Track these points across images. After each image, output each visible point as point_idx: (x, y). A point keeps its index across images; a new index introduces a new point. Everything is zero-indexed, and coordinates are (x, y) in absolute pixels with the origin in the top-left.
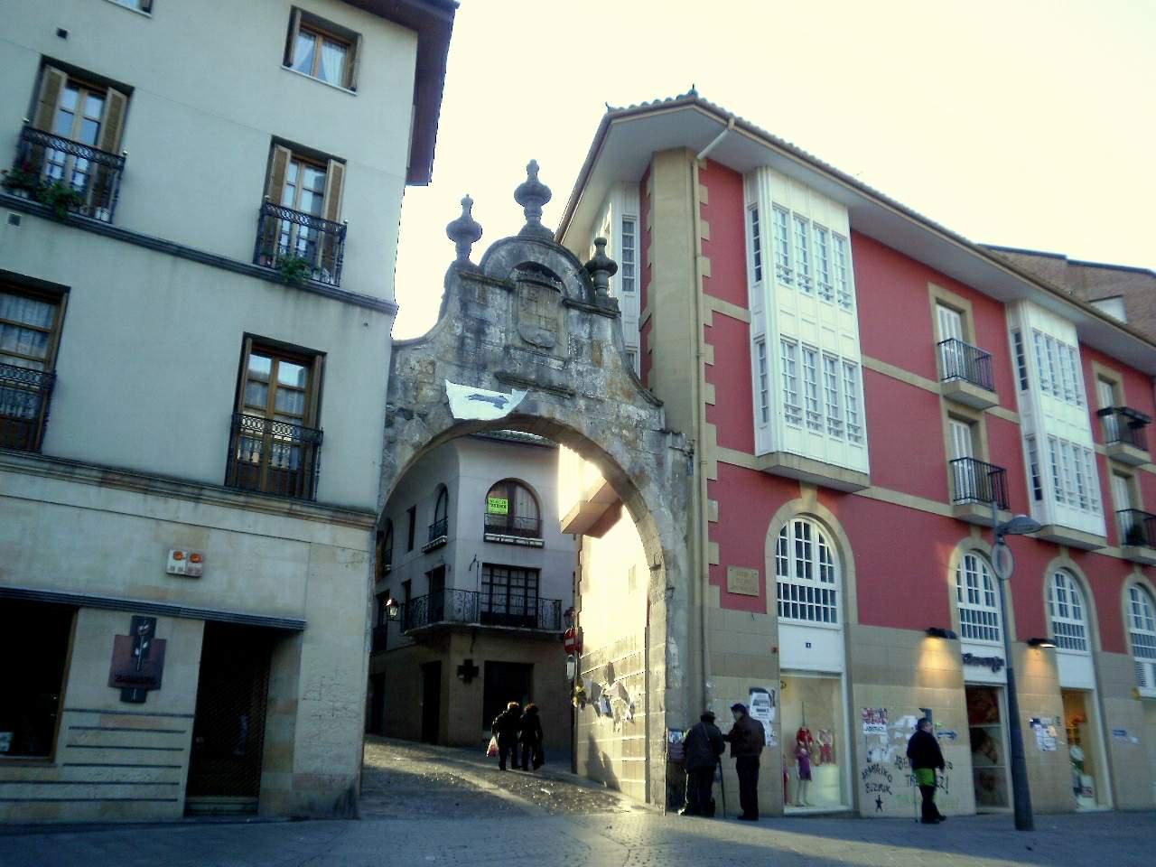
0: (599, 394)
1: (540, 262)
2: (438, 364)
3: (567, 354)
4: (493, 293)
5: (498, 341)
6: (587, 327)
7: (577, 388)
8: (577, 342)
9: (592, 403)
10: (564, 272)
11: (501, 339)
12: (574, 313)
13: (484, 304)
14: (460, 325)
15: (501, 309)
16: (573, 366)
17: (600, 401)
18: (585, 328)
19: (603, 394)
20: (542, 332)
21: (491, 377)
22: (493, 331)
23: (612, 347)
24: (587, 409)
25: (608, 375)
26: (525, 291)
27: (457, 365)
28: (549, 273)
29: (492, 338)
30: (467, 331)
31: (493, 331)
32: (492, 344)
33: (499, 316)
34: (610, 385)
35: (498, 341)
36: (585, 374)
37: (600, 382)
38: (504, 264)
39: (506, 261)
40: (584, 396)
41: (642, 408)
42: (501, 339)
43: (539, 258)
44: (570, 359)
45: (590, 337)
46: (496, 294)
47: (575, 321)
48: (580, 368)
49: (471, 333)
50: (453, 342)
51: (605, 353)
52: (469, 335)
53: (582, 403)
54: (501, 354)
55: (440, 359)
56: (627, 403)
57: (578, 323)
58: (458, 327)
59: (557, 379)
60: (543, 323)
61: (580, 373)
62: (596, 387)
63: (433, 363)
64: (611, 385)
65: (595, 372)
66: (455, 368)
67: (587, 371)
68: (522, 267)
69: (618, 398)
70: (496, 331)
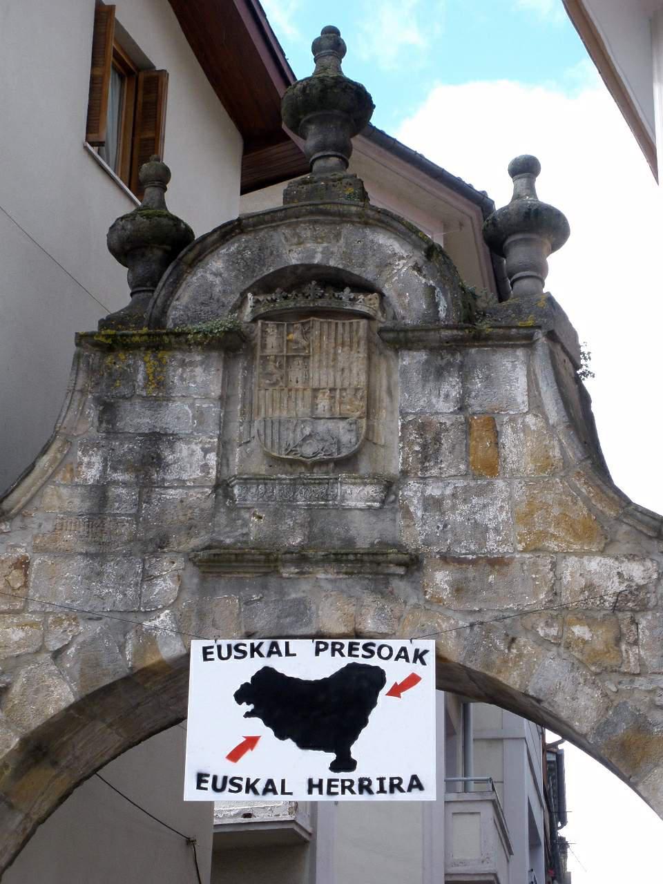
0: (493, 545)
1: (317, 260)
2: (36, 562)
3: (395, 466)
4: (183, 364)
5: (198, 474)
6: (452, 386)
7: (427, 543)
8: (422, 428)
9: (471, 572)
10: (386, 264)
11: (205, 468)
12: (412, 360)
13: (160, 392)
14: (97, 460)
15: (206, 397)
16: (411, 491)
17: (497, 563)
18: (445, 388)
19: (504, 542)
20: (322, 427)
21: (180, 563)
22: (185, 453)
23: (530, 420)
24: (459, 590)
25: (519, 491)
26: (272, 339)
27: (86, 554)
28: (334, 280)
29: (182, 469)
30: (115, 469)
31: (185, 453)
32: (182, 484)
33: (200, 416)
34: (524, 518)
35: (198, 474)
36: (448, 503)
37: (495, 513)
39: (224, 282)
40: (447, 559)
41: (632, 557)
42: (205, 468)
44: (405, 473)
45: (462, 408)
46: (191, 363)
47: (415, 377)
48: (434, 490)
49: (126, 470)
50: (77, 501)
51: (508, 438)
52: (118, 476)
53: (441, 578)
54: (209, 504)
55: (38, 549)
56: (580, 554)
57: (425, 380)
58: (90, 465)
59: (365, 532)
60: (323, 404)
61: (433, 504)
62: (487, 529)
63: (23, 565)
64: (530, 514)
65: (481, 492)
66: (80, 563)
67: (454, 495)
68: (265, 286)
69: (552, 545)
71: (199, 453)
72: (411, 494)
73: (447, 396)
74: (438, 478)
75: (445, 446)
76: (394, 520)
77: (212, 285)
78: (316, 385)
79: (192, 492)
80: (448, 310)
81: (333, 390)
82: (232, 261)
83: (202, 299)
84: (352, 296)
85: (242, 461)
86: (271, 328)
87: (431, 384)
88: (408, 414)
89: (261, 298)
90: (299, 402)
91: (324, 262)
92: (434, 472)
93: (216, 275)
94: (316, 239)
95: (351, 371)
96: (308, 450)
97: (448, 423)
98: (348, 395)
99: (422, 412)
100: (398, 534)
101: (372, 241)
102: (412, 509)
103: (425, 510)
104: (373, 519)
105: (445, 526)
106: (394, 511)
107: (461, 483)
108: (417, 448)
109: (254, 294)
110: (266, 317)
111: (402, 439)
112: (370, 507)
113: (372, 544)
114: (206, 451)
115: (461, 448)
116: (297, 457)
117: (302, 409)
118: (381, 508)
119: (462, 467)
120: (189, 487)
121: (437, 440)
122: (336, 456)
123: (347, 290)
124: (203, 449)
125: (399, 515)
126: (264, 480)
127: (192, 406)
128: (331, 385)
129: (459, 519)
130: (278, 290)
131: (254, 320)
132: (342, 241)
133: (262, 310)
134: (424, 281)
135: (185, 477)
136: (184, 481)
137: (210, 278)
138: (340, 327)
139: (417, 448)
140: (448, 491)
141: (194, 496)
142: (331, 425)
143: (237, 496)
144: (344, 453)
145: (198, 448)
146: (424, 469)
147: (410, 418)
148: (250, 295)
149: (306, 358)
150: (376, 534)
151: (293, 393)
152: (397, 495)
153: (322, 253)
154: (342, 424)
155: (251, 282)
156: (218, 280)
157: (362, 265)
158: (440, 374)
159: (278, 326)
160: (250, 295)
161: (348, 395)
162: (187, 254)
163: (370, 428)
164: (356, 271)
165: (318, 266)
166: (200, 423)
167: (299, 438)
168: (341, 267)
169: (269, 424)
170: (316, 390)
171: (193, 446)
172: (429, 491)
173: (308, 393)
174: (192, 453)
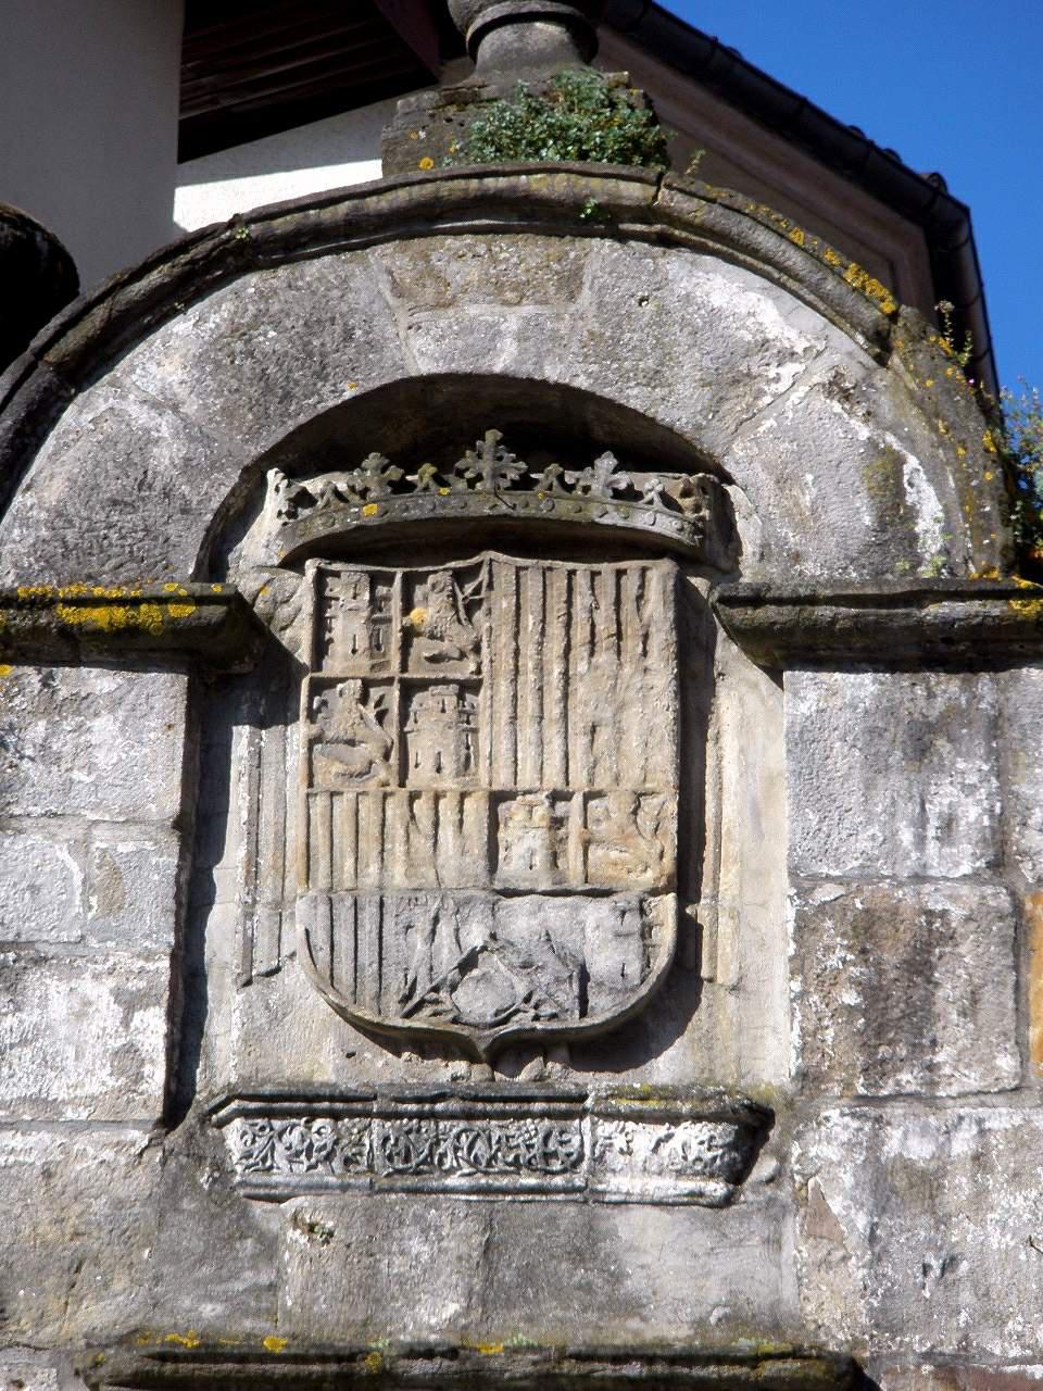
1: (504, 360)
5: (103, 1081)
8: (866, 930)
11: (127, 1057)
15: (132, 819)
18: (944, 795)
22: (59, 1007)
33: (110, 884)
36: (960, 1185)
38: (166, 455)
39: (190, 431)
43: (495, 333)
45: (1000, 860)
48: (907, 1142)
54: (143, 1181)
57: (876, 767)
60: (523, 843)
70: (83, 1011)
71: (107, 1013)
72: (832, 1152)
73: (948, 824)
74: (927, 1099)
75: (949, 992)
76: (774, 1242)
77: (147, 440)
78: (503, 781)
79: (81, 1142)
80: (946, 530)
81: (556, 797)
82: (211, 359)
83: (112, 488)
84: (623, 480)
85: (250, 1038)
86: (348, 584)
87: (897, 781)
88: (818, 880)
89: (314, 485)
90: (447, 833)
91: (526, 370)
92: (909, 1079)
93: (165, 403)
94: (499, 290)
95: (619, 732)
96: (476, 1002)
97: (957, 913)
98: (612, 809)
99: (867, 877)
100: (788, 1291)
101: (688, 299)
102: (836, 1205)
103: (881, 1208)
104: (702, 1240)
105: (950, 1264)
106: (774, 1212)
107: (1001, 1119)
108: (850, 998)
109: (292, 474)
110: (337, 548)
111: (798, 965)
112: (695, 1197)
113: (700, 1324)
114: (131, 1003)
115: (1000, 1000)
116: (441, 1024)
117: (457, 855)
118: (728, 1201)
119: (1006, 1063)
120: (76, 1127)
121: (920, 966)
122: (574, 1021)
123: (607, 462)
124: (118, 994)
125: (792, 1228)
126: (342, 1104)
127: (81, 847)
128: (553, 780)
129: (996, 1240)
130: (373, 460)
131: (293, 562)
132: (586, 296)
133: (319, 528)
134: (864, 433)
135: (58, 1091)
136: (54, 1105)
137: (141, 416)
138: (581, 581)
139: (850, 998)
140: (963, 1144)
141: (92, 1155)
142: (556, 913)
143: (235, 1159)
144: (604, 1008)
145: (100, 992)
146: (876, 1069)
147: (827, 893)
148: (273, 477)
149: (469, 687)
150: (715, 1292)
151: (422, 807)
152: (783, 1158)
153: (521, 337)
154: (596, 914)
155: (278, 434)
156: (165, 425)
157: (654, 378)
158: (922, 743)
159: (375, 580)
160: (273, 477)
161: (612, 809)
162: (66, 337)
163: (689, 933)
164: (635, 397)
165: (504, 380)
166: (112, 906)
167: (447, 959)
168: (582, 383)
169: (344, 914)
170: (497, 798)
171: (87, 986)
172: (893, 1143)
173: (476, 808)
174: (83, 1011)
